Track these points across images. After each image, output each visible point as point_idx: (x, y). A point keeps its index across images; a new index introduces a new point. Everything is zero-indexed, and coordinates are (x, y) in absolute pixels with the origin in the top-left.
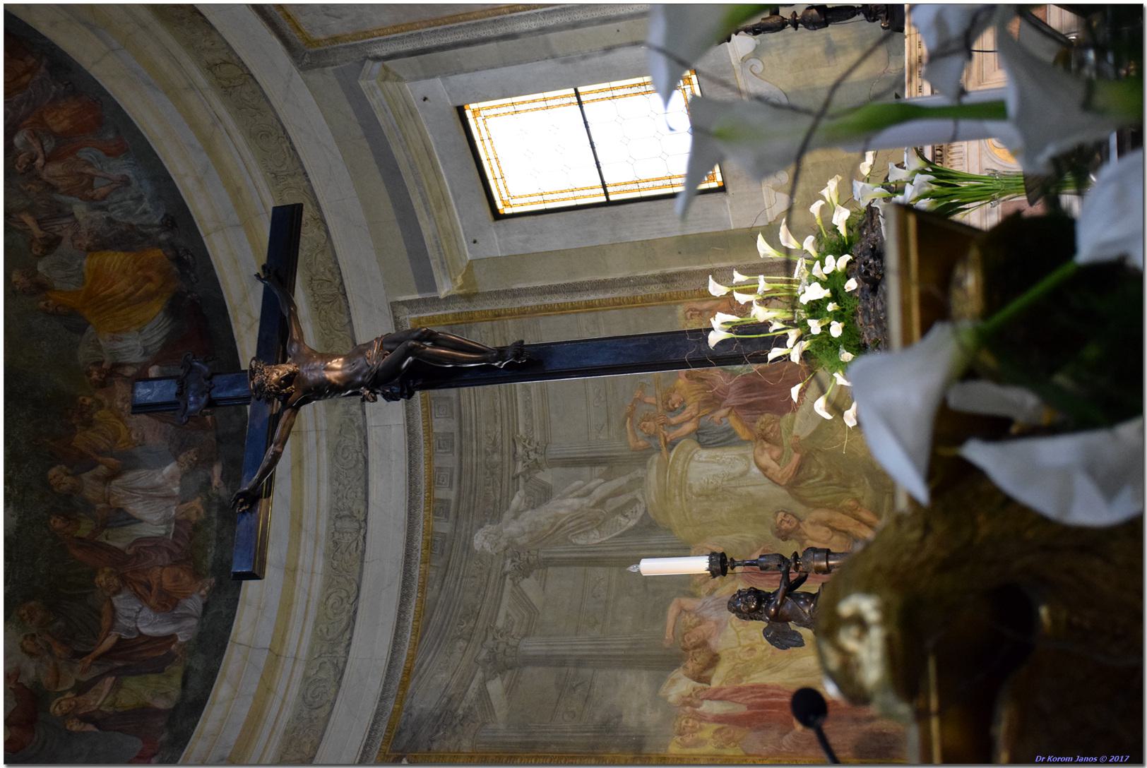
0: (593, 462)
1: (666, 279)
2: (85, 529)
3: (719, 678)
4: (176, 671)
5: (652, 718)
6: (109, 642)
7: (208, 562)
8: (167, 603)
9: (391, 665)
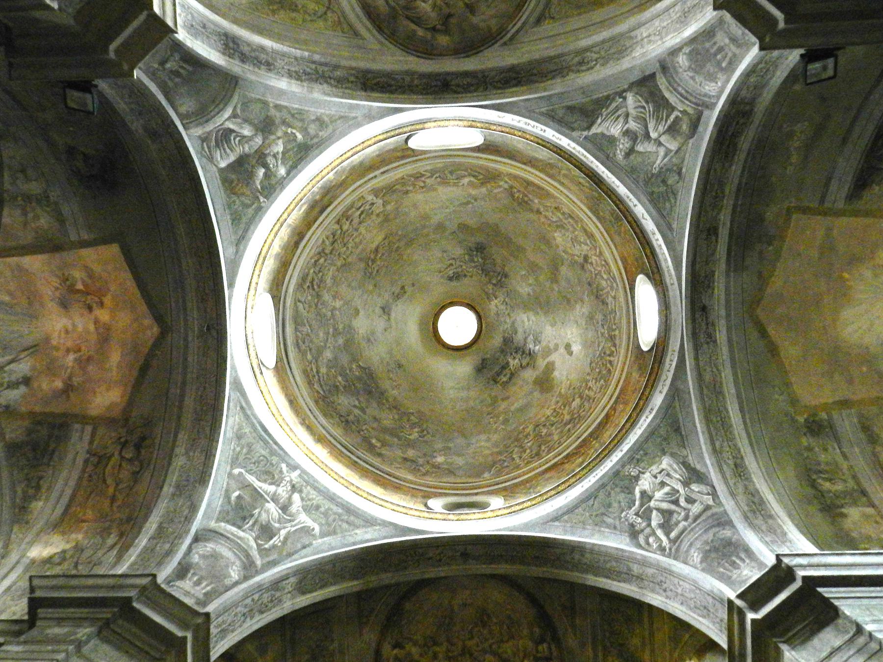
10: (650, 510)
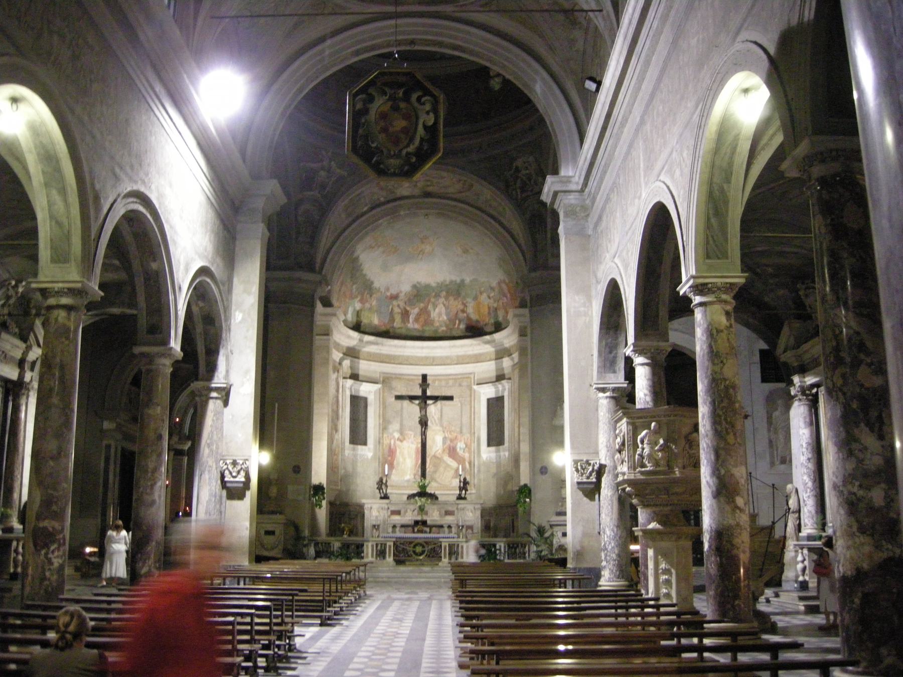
0: (441, 416)
1: (474, 433)
2: (433, 300)
3: (398, 443)
4: (402, 325)
5: (391, 430)
6: (408, 309)
7: (425, 328)
8: (416, 320)
9: (402, 375)
10: (517, 177)
